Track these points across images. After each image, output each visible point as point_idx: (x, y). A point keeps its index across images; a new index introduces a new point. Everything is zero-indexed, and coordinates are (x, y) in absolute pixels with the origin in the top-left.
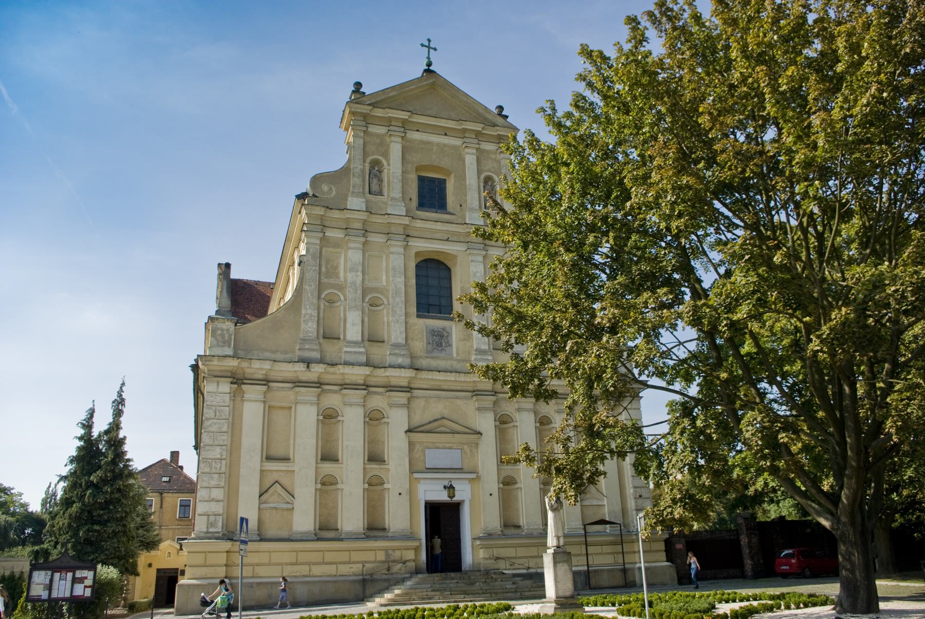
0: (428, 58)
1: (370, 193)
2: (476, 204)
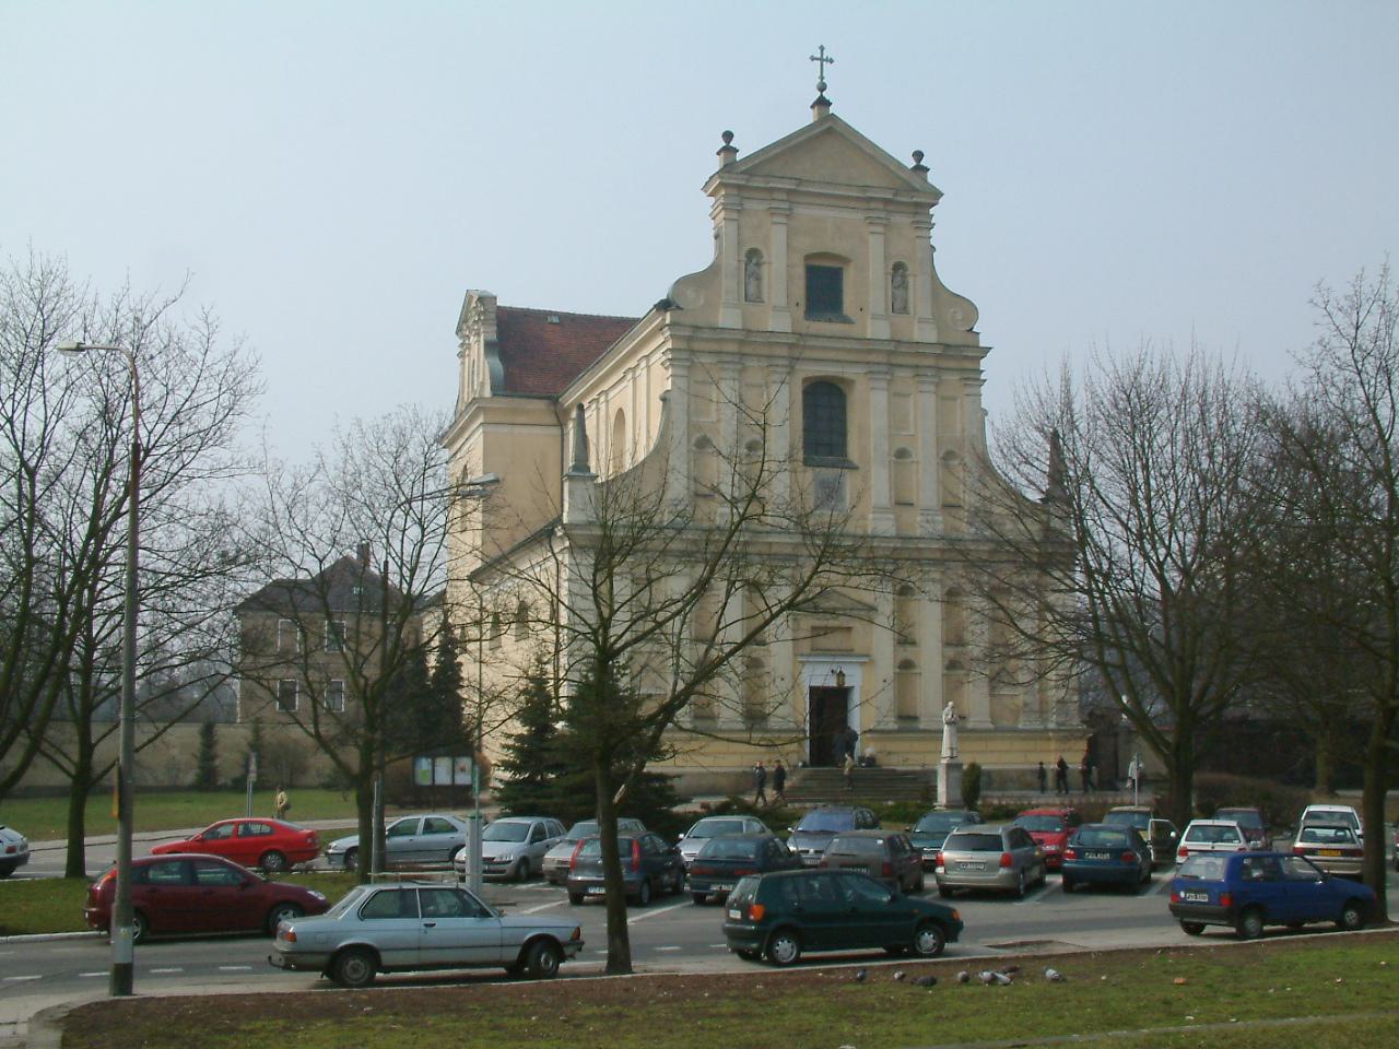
0: (822, 78)
1: (746, 300)
2: (880, 309)
